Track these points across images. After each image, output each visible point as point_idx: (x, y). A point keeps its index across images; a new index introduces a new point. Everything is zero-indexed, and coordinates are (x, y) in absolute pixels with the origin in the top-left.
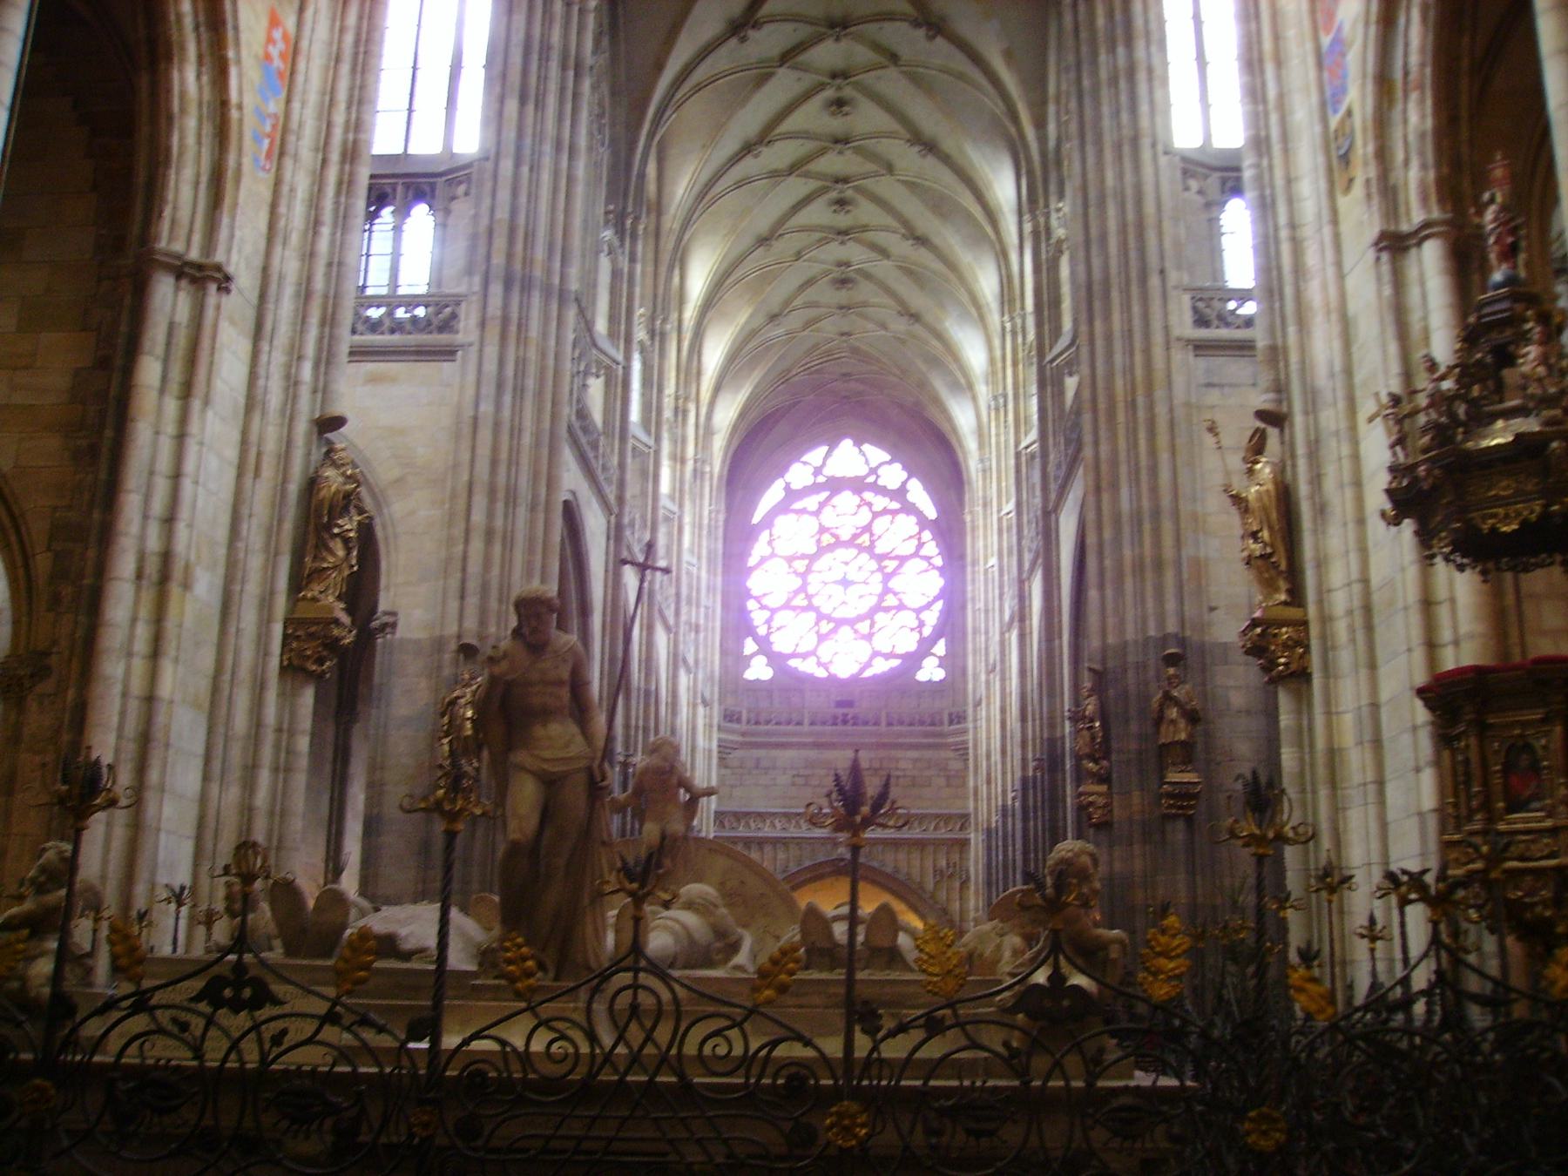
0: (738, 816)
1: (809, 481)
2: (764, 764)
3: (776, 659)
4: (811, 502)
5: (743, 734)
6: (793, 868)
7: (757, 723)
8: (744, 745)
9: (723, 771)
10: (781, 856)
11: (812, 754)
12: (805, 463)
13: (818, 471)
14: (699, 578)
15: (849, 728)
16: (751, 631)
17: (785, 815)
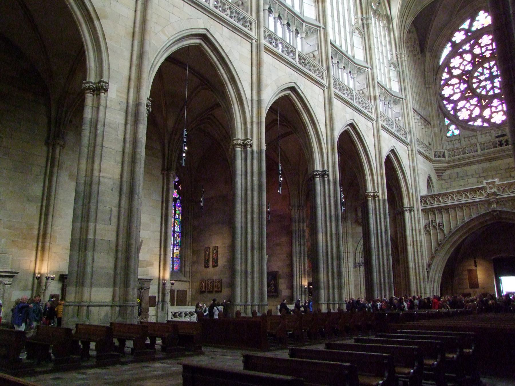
0: (433, 197)
1: (464, 37)
2: (461, 175)
3: (462, 125)
4: (467, 47)
5: (448, 162)
6: (466, 219)
7: (455, 156)
8: (449, 168)
9: (441, 182)
10: (459, 214)
11: (486, 165)
12: (459, 31)
13: (467, 31)
14: (373, 74)
15: (504, 147)
16: (446, 114)
17: (458, 192)
